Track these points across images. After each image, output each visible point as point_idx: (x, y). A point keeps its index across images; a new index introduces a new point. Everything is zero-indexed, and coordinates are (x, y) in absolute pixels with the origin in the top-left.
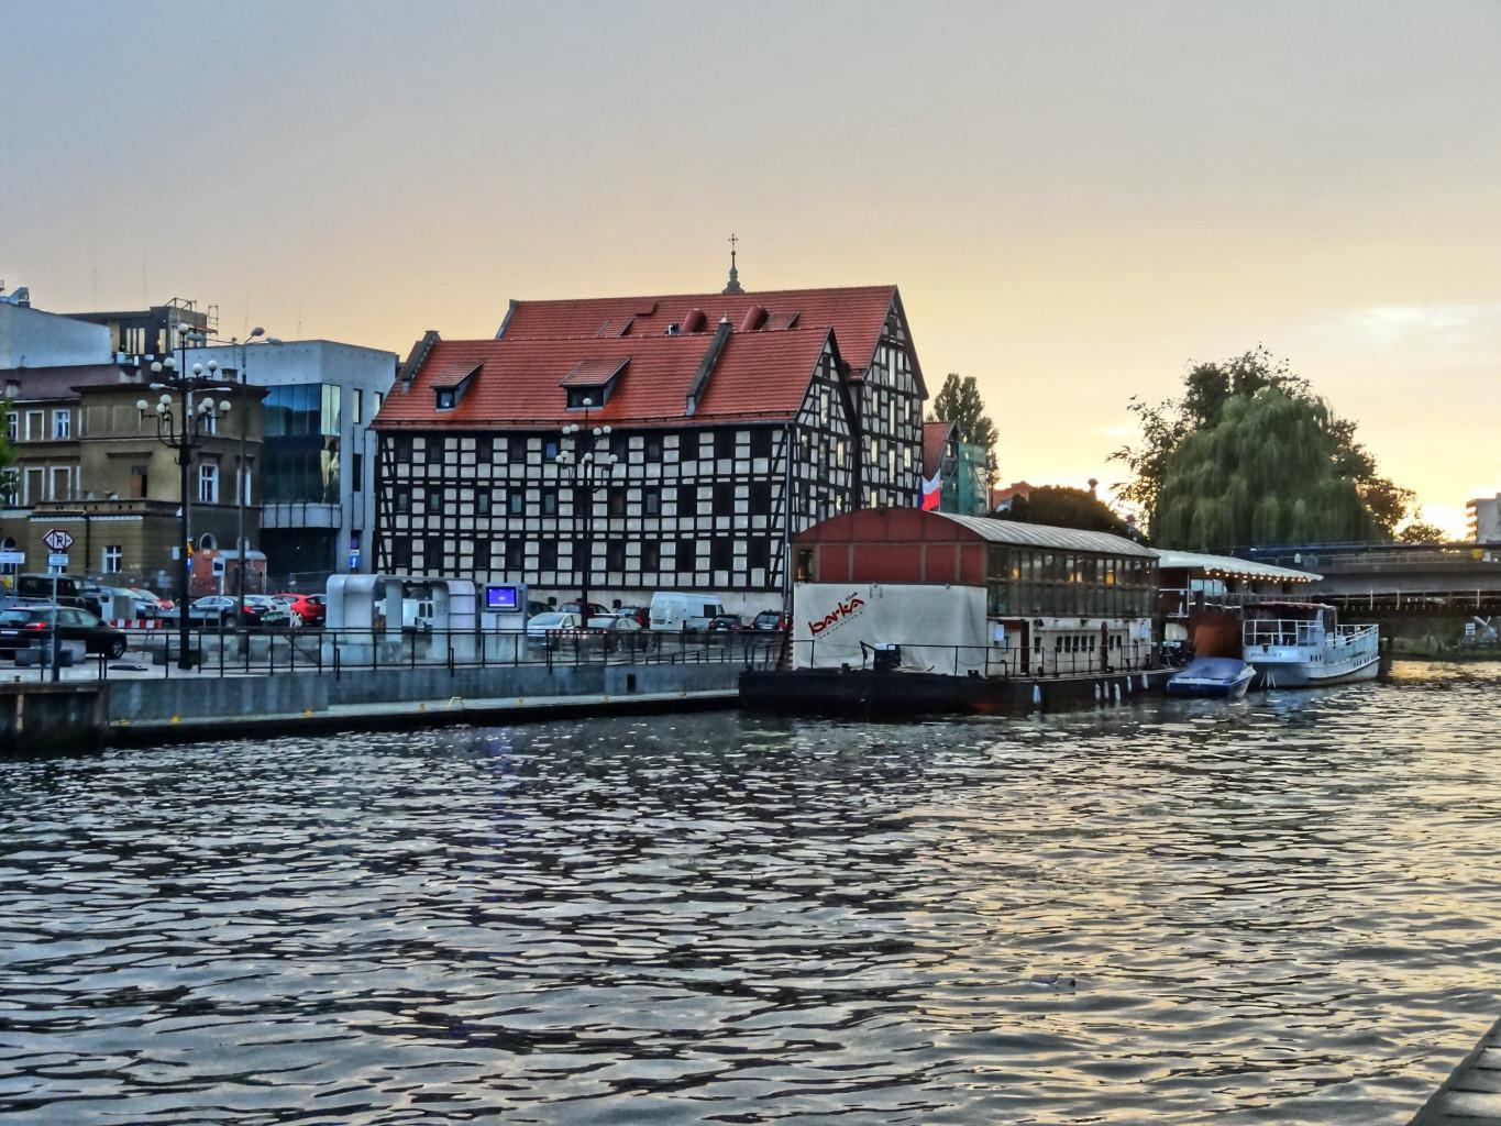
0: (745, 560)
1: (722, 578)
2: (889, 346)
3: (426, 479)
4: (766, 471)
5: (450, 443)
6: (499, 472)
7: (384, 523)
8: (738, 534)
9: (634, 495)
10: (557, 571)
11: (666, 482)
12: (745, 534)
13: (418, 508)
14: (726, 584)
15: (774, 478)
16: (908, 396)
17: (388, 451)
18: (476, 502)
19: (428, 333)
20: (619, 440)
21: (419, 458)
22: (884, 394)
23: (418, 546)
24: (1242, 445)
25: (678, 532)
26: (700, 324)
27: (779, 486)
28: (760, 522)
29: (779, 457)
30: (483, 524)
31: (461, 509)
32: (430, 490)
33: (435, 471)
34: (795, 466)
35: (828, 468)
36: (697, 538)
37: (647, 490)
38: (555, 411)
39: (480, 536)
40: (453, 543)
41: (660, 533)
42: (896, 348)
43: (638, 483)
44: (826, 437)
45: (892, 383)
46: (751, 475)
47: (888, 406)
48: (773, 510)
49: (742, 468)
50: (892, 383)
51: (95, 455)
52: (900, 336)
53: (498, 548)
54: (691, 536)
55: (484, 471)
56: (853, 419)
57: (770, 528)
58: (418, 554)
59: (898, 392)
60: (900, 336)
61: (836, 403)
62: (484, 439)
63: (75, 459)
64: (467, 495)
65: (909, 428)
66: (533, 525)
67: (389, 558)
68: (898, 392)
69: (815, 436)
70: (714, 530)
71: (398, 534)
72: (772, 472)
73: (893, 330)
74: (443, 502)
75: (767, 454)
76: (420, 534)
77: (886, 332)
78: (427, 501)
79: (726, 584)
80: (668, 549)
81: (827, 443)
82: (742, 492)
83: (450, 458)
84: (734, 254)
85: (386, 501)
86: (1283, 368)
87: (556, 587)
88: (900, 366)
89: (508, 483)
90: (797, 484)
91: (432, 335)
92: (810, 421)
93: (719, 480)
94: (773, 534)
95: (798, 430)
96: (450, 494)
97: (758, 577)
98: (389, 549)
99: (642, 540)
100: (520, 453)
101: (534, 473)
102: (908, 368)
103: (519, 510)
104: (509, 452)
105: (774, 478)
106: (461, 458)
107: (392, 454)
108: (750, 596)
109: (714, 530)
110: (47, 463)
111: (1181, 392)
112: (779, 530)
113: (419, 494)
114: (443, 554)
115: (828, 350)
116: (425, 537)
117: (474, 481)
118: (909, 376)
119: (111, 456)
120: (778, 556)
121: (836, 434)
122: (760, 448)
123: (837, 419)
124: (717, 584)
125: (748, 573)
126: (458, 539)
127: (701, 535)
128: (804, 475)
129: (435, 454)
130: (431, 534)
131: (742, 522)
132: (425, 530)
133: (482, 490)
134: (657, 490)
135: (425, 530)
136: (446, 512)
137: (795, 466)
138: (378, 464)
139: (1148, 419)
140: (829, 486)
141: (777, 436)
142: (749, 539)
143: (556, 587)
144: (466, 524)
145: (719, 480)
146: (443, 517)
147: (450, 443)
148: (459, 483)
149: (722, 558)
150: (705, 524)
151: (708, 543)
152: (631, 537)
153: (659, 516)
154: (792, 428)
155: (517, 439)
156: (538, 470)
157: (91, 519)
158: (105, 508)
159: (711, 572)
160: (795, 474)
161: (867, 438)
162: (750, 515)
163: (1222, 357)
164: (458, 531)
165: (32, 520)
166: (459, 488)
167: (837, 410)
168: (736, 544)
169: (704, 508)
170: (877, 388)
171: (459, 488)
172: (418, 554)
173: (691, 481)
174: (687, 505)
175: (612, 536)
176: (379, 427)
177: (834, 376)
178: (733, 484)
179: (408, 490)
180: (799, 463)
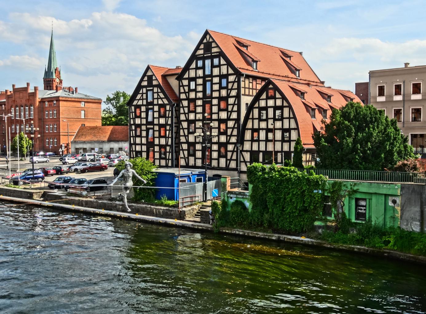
42: (212, 58)
69: (143, 109)
92: (140, 103)
95: (133, 108)
102: (223, 62)
121: (158, 104)
123: (158, 99)
167: (158, 95)
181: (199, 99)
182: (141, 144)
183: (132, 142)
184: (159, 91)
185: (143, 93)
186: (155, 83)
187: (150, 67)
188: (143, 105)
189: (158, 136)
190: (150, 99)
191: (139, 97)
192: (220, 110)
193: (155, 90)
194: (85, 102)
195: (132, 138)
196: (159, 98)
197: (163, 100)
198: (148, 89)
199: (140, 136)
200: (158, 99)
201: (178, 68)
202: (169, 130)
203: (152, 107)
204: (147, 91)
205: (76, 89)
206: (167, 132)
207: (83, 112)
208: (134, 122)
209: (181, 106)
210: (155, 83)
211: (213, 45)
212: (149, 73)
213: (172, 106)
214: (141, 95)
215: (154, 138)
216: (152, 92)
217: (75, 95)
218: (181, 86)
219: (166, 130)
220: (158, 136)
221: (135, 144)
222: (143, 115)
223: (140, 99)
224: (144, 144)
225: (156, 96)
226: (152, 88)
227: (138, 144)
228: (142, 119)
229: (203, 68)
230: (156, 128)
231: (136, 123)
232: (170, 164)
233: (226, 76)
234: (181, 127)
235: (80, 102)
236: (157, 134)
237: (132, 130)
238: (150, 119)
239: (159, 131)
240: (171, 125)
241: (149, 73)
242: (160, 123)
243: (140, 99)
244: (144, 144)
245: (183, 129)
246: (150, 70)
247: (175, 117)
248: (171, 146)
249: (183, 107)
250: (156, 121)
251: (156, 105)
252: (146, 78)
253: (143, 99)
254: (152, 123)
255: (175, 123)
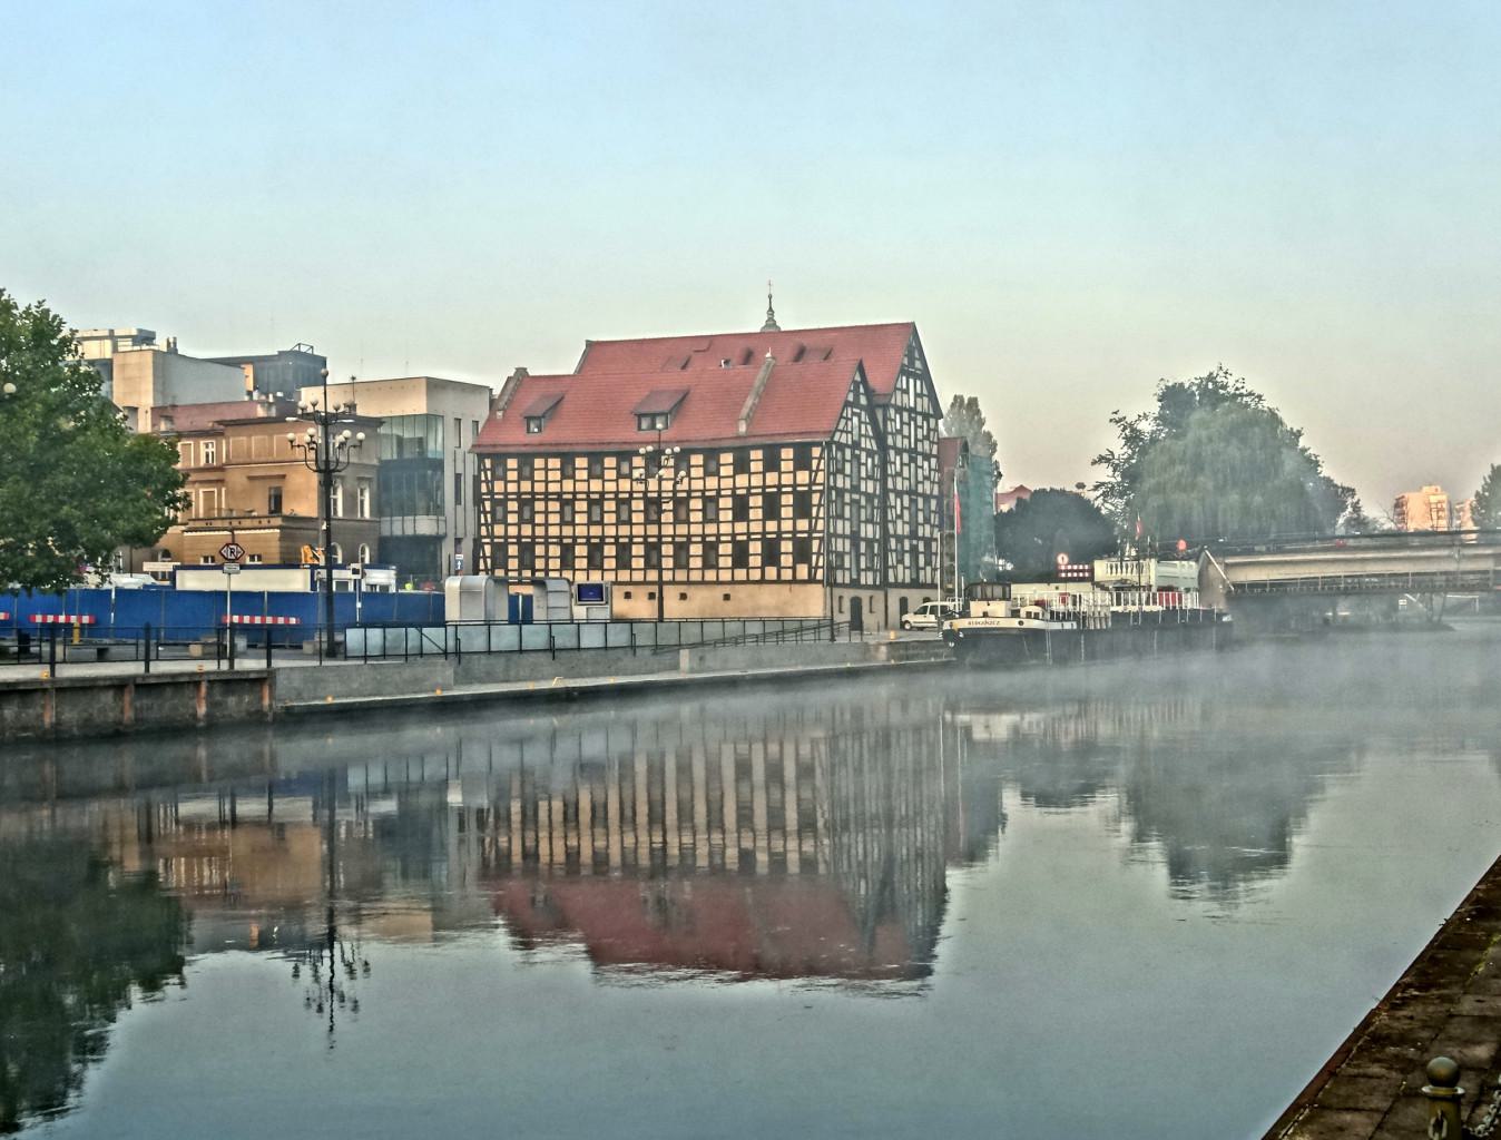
0: (790, 558)
1: (771, 572)
2: (909, 375)
3: (519, 494)
4: (807, 481)
5: (539, 463)
6: (581, 487)
7: (484, 531)
8: (784, 536)
9: (696, 504)
10: (632, 570)
11: (723, 493)
12: (790, 535)
13: (512, 518)
14: (775, 578)
15: (814, 488)
16: (926, 416)
17: (485, 470)
18: (561, 512)
19: (517, 369)
20: (682, 459)
21: (512, 476)
22: (905, 415)
23: (513, 550)
24: (1207, 450)
25: (734, 535)
26: (748, 357)
27: (818, 495)
28: (803, 524)
29: (818, 470)
30: (567, 531)
31: (549, 520)
32: (522, 503)
33: (526, 486)
34: (832, 477)
35: (860, 478)
36: (749, 539)
37: (706, 500)
38: (625, 433)
39: (565, 541)
40: (543, 547)
41: (718, 536)
42: (916, 377)
43: (699, 494)
44: (857, 452)
45: (912, 405)
46: (795, 485)
47: (909, 425)
48: (814, 514)
49: (787, 479)
50: (912, 405)
51: (237, 478)
52: (918, 364)
53: (581, 550)
54: (745, 538)
55: (568, 485)
56: (880, 437)
57: (811, 530)
58: (512, 557)
59: (917, 413)
60: (918, 364)
61: (866, 423)
62: (567, 459)
63: (221, 482)
64: (554, 506)
65: (926, 443)
66: (611, 531)
67: (489, 561)
68: (917, 413)
70: (764, 533)
71: (496, 540)
72: (812, 483)
73: (912, 363)
74: (533, 513)
75: (807, 467)
76: (514, 540)
77: (906, 362)
78: (520, 512)
79: (775, 578)
80: (725, 549)
81: (858, 457)
82: (787, 500)
83: (539, 475)
84: (770, 297)
85: (485, 513)
86: (1239, 385)
87: (631, 583)
88: (919, 391)
89: (588, 496)
90: (834, 493)
91: (521, 372)
92: (843, 440)
93: (768, 490)
94: (815, 535)
96: (539, 506)
97: (803, 571)
98: (488, 553)
99: (703, 542)
100: (598, 468)
101: (610, 487)
102: (925, 392)
103: (599, 519)
104: (589, 469)
105: (814, 488)
106: (548, 474)
107: (489, 473)
108: (796, 587)
109: (764, 533)
110: (197, 485)
111: (1154, 407)
112: (819, 532)
113: (513, 506)
114: (534, 557)
115: (858, 378)
116: (519, 543)
117: (560, 494)
118: (926, 399)
119: (251, 478)
120: (819, 554)
121: (865, 449)
122: (802, 462)
123: (866, 436)
124: (767, 578)
125: (794, 569)
126: (547, 544)
127: (753, 537)
128: (840, 484)
129: (526, 472)
130: (523, 540)
131: (787, 526)
132: (519, 537)
133: (567, 503)
134: (715, 500)
135: (519, 537)
136: (537, 521)
137: (832, 477)
138: (477, 481)
139: (1127, 431)
140: (861, 493)
141: (816, 452)
142: (794, 539)
143: (631, 583)
144: (554, 531)
145: (768, 490)
146: (534, 525)
147: (539, 463)
148: (547, 496)
149: (771, 555)
150: (756, 527)
151: (759, 544)
152: (694, 539)
153: (717, 521)
154: (829, 445)
155: (596, 458)
156: (614, 484)
157: (236, 532)
158: (247, 523)
159: (762, 568)
160: (832, 484)
161: (892, 453)
162: (794, 519)
163: (1189, 374)
164: (546, 537)
165: (186, 534)
166: (546, 500)
168: (783, 543)
169: (756, 514)
170: (900, 410)
171: (546, 500)
172: (512, 557)
173: (744, 492)
174: (741, 511)
175: (677, 539)
176: (478, 450)
177: (863, 400)
178: (780, 493)
179: (504, 503)
180: (835, 475)
181: (905, 451)
182: (843, 536)
183: (832, 531)
188: (847, 445)
192: (925, 478)
193: (863, 413)
198: (855, 410)
211: (917, 355)
221: (837, 536)
226: (858, 411)
229: (906, 392)
233: (926, 416)
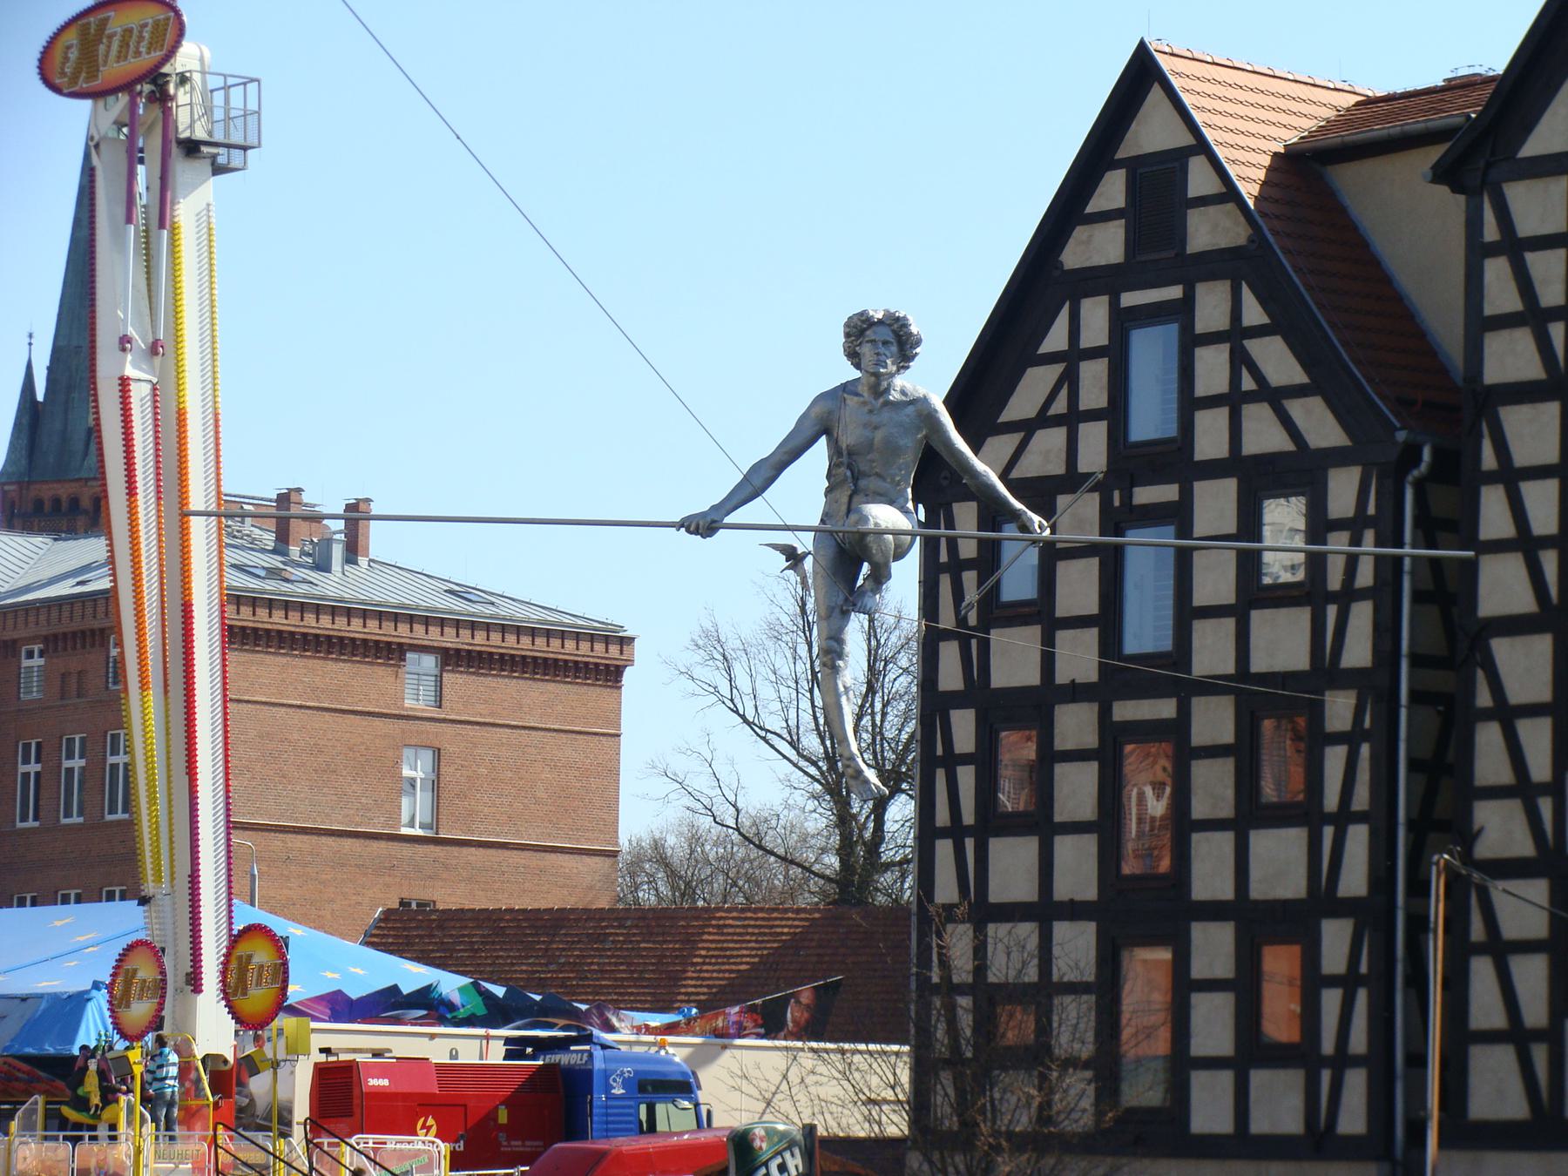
34: (949, 653)
61: (1236, 335)
121: (1235, 464)
137: (949, 653)
167: (1241, 360)
182: (1045, 910)
184: (1253, 313)
185: (1073, 356)
186: (1207, 231)
187: (1165, 63)
189: (1226, 810)
190: (1150, 418)
191: (1032, 391)
194: (451, 659)
195: (944, 848)
196: (1251, 397)
197: (1295, 408)
198: (1129, 299)
199: (1040, 823)
200: (1233, 401)
201: (1459, 86)
202: (1351, 739)
203: (1167, 493)
204: (1123, 322)
205: (356, 515)
206: (1335, 758)
207: (416, 768)
208: (977, 667)
209: (1489, 460)
210: (1207, 231)
212: (1152, 132)
213: (1388, 473)
214: (1058, 369)
215: (1182, 825)
216: (1172, 330)
217: (337, 584)
218: (1492, 250)
219: (1316, 740)
220: (1226, 810)
222: (1078, 589)
223: (1043, 420)
224: (1075, 911)
225: (1212, 369)
226: (1175, 292)
227: (1011, 912)
228: (1062, 636)
230: (1214, 721)
231: (999, 679)
232: (1353, 1119)
234: (1484, 699)
235: (392, 653)
236: (1213, 788)
237: (952, 761)
238: (1146, 630)
239: (1245, 753)
240: (1375, 685)
241: (1152, 132)
242: (1258, 664)
243: (1043, 420)
244: (1075, 911)
245: (1507, 715)
246: (1156, 93)
247: (1417, 597)
248: (1371, 915)
249: (1511, 477)
250: (1212, 651)
251: (1213, 469)
252: (1112, 191)
253: (1073, 419)
254: (1169, 672)
255: (1417, 661)
